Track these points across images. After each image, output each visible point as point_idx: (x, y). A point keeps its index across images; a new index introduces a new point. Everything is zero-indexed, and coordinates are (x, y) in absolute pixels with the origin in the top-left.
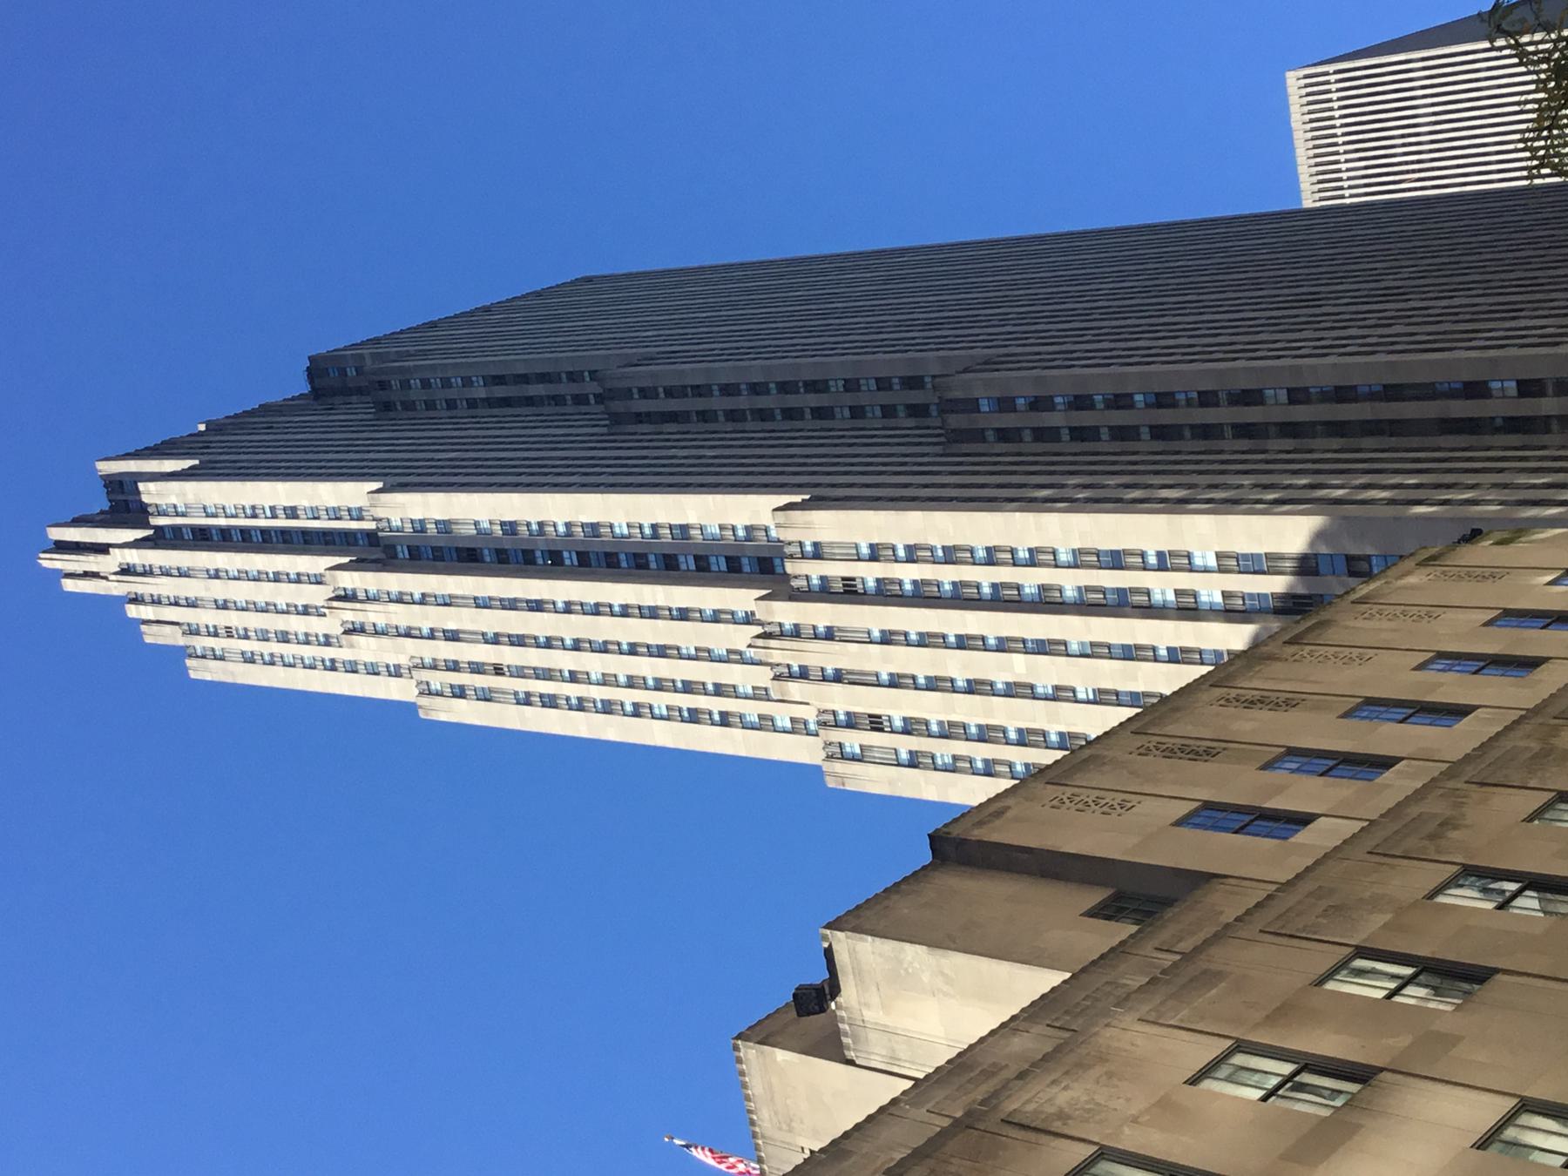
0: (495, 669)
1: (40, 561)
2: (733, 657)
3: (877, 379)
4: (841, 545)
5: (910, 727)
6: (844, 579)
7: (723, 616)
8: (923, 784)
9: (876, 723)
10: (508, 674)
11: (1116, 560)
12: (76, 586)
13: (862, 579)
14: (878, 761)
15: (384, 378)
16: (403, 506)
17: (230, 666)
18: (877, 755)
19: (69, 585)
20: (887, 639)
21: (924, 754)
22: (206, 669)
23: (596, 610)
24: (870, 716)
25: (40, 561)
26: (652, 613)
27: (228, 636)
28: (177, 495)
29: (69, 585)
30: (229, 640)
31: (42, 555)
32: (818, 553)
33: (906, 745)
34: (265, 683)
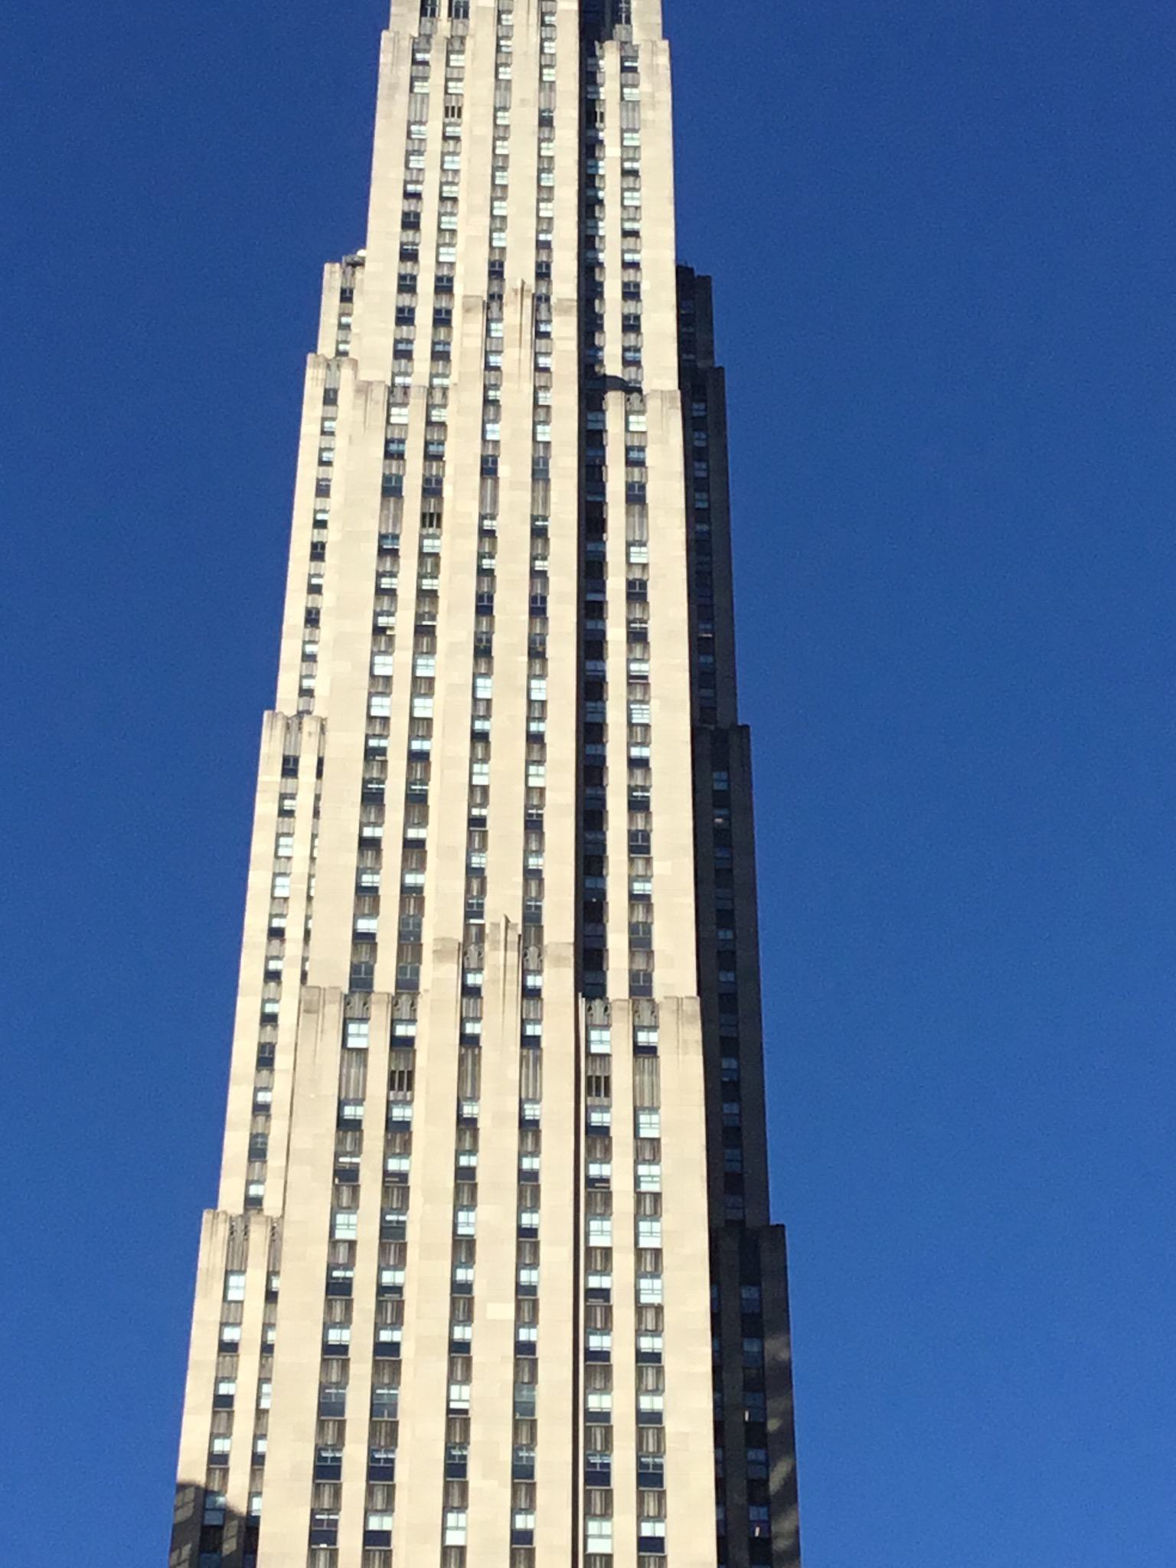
0: (432, 515)
4: (654, 1086)
5: (398, 1133)
6: (607, 1079)
7: (533, 885)
9: (401, 1080)
10: (425, 532)
14: (344, 1071)
17: (403, 97)
18: (353, 1071)
21: (358, 1143)
22: (395, 62)
27: (447, 109)
32: (644, 1053)
33: (372, 1116)
34: (379, 143)
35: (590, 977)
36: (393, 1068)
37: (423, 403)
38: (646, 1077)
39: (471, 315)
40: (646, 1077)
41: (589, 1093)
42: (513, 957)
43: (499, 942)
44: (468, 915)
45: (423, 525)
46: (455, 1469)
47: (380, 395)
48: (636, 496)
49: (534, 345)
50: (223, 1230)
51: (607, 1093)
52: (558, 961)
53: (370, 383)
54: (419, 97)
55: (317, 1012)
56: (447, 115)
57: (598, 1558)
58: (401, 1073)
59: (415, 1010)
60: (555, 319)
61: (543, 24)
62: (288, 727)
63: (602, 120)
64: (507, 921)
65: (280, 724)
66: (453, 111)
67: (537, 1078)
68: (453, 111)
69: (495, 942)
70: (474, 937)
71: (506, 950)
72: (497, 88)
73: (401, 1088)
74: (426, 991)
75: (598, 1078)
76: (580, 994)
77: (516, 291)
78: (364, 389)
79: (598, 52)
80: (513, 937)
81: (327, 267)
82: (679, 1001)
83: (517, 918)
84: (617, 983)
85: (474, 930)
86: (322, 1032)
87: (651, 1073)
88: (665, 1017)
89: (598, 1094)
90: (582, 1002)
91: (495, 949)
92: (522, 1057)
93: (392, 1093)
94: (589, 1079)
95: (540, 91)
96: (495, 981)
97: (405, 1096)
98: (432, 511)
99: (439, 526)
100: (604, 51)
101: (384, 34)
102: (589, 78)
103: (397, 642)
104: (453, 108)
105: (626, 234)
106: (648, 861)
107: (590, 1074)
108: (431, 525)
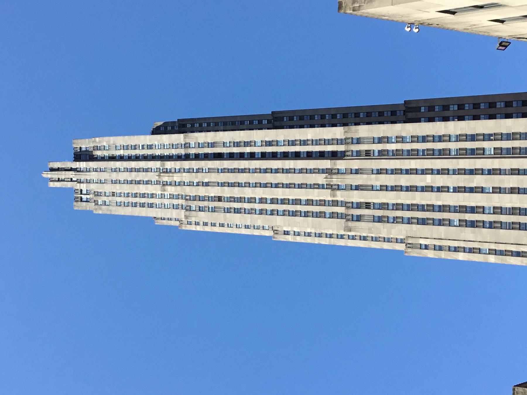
0: (219, 199)
1: (42, 175)
2: (316, 186)
3: (379, 112)
4: (367, 138)
6: (366, 151)
8: (382, 229)
10: (223, 201)
11: (473, 138)
12: (54, 184)
13: (374, 150)
15: (184, 123)
16: (197, 138)
17: (110, 208)
18: (366, 218)
19: (52, 185)
20: (379, 172)
23: (266, 171)
24: (366, 203)
25: (42, 175)
26: (288, 171)
27: (113, 196)
28: (106, 142)
29: (52, 185)
30: (114, 197)
31: (44, 173)
35: (339, 155)
36: (365, 208)
37: (189, 202)
38: (365, 140)
39: (166, 189)
40: (365, 140)
41: (370, 156)
42: (334, 176)
43: (330, 180)
44: (323, 188)
45: (221, 201)
46: (472, 190)
47: (188, 213)
48: (213, 145)
49: (173, 173)
50: (409, 250)
51: (370, 151)
52: (335, 164)
53: (185, 216)
54: (110, 203)
55: (351, 228)
56: (115, 196)
57: (495, 151)
58: (366, 206)
59: (350, 202)
60: (166, 167)
61: (89, 171)
62: (276, 233)
63: (114, 155)
64: (325, 178)
65: (276, 236)
66: (113, 194)
67: (366, 170)
68: (113, 194)
69: (330, 181)
70: (330, 187)
71: (332, 178)
72: (107, 183)
73: (370, 206)
74: (344, 199)
75: (366, 153)
76: (344, 158)
77: (159, 178)
78: (186, 217)
79: (96, 156)
80: (329, 177)
81: (156, 224)
82: (346, 132)
83: (324, 175)
84: (341, 148)
85: (328, 187)
86: (356, 227)
87: (364, 139)
88: (349, 135)
89: (370, 153)
90: (345, 158)
91: (332, 181)
92: (361, 174)
93: (371, 208)
94: (366, 156)
95: (107, 172)
96: (341, 181)
97: (372, 204)
98: (218, 199)
99: (221, 197)
100: (96, 155)
101: (95, 212)
102: (103, 159)
103: (252, 207)
104: (112, 194)
105: (143, 148)
106: (308, 140)
107: (365, 156)
108: (221, 199)
